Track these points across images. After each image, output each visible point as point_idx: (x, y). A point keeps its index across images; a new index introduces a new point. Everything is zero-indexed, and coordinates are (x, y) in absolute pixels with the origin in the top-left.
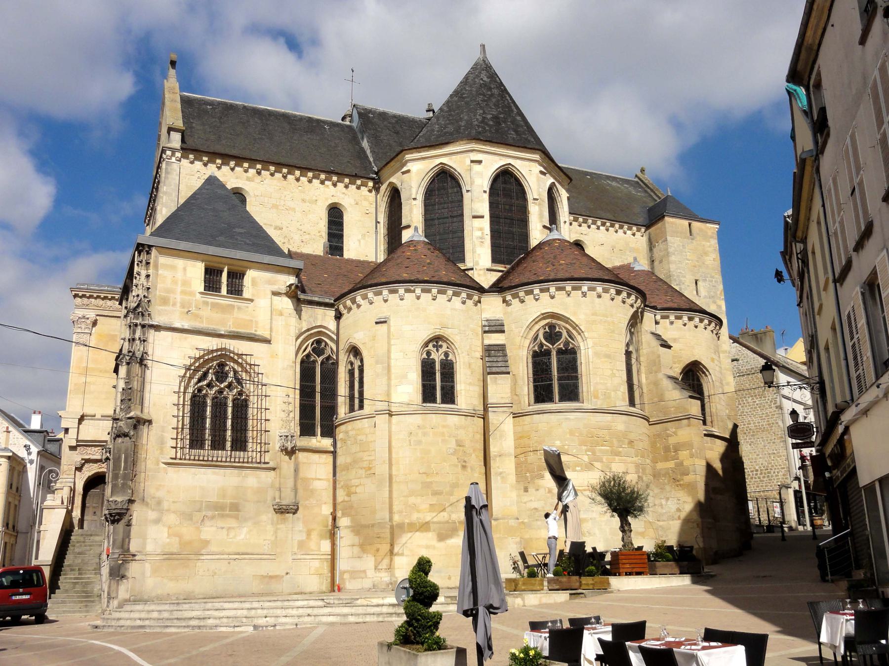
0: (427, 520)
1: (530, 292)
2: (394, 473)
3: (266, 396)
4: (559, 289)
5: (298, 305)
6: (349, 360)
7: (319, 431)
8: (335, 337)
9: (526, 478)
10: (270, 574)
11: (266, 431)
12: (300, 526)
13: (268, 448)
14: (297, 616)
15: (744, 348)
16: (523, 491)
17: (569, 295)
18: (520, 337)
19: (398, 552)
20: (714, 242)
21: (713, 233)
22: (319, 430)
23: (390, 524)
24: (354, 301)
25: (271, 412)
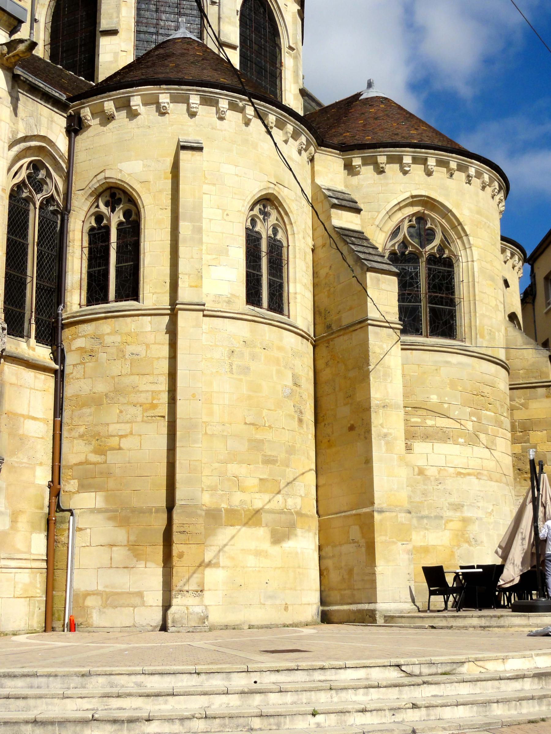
1: (398, 160)
5: (13, 87)
6: (93, 210)
8: (64, 166)
14: (391, 709)
17: (451, 175)
19: (210, 562)
22: (33, 327)
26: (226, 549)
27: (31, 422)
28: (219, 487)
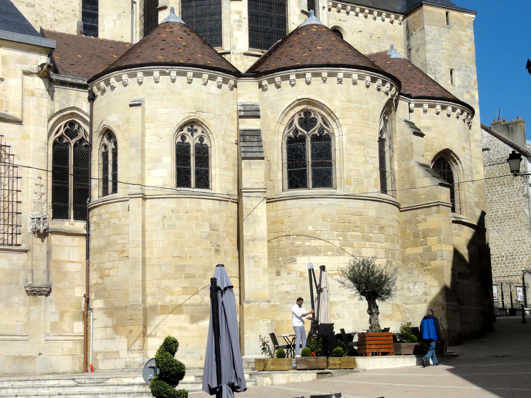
0: (180, 303)
2: (148, 256)
3: (17, 178)
4: (315, 75)
5: (50, 86)
6: (102, 143)
7: (72, 213)
8: (88, 119)
9: (279, 262)
10: (23, 355)
11: (17, 213)
12: (53, 308)
13: (20, 230)
15: (495, 138)
16: (275, 275)
17: (324, 81)
18: (275, 123)
19: (151, 334)
20: (470, 32)
21: (469, 22)
23: (143, 306)
24: (108, 83)
25: (23, 194)
26: (160, 327)
27: (70, 264)
28: (157, 293)
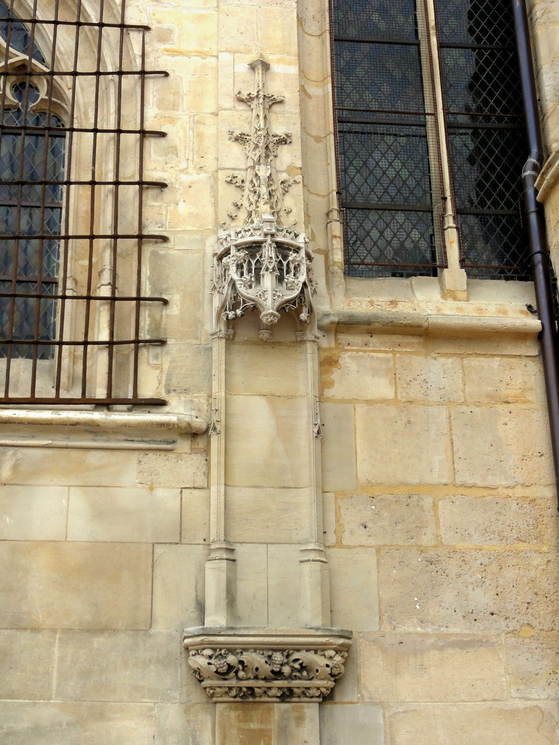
13: (156, 325)
25: (174, 150)
